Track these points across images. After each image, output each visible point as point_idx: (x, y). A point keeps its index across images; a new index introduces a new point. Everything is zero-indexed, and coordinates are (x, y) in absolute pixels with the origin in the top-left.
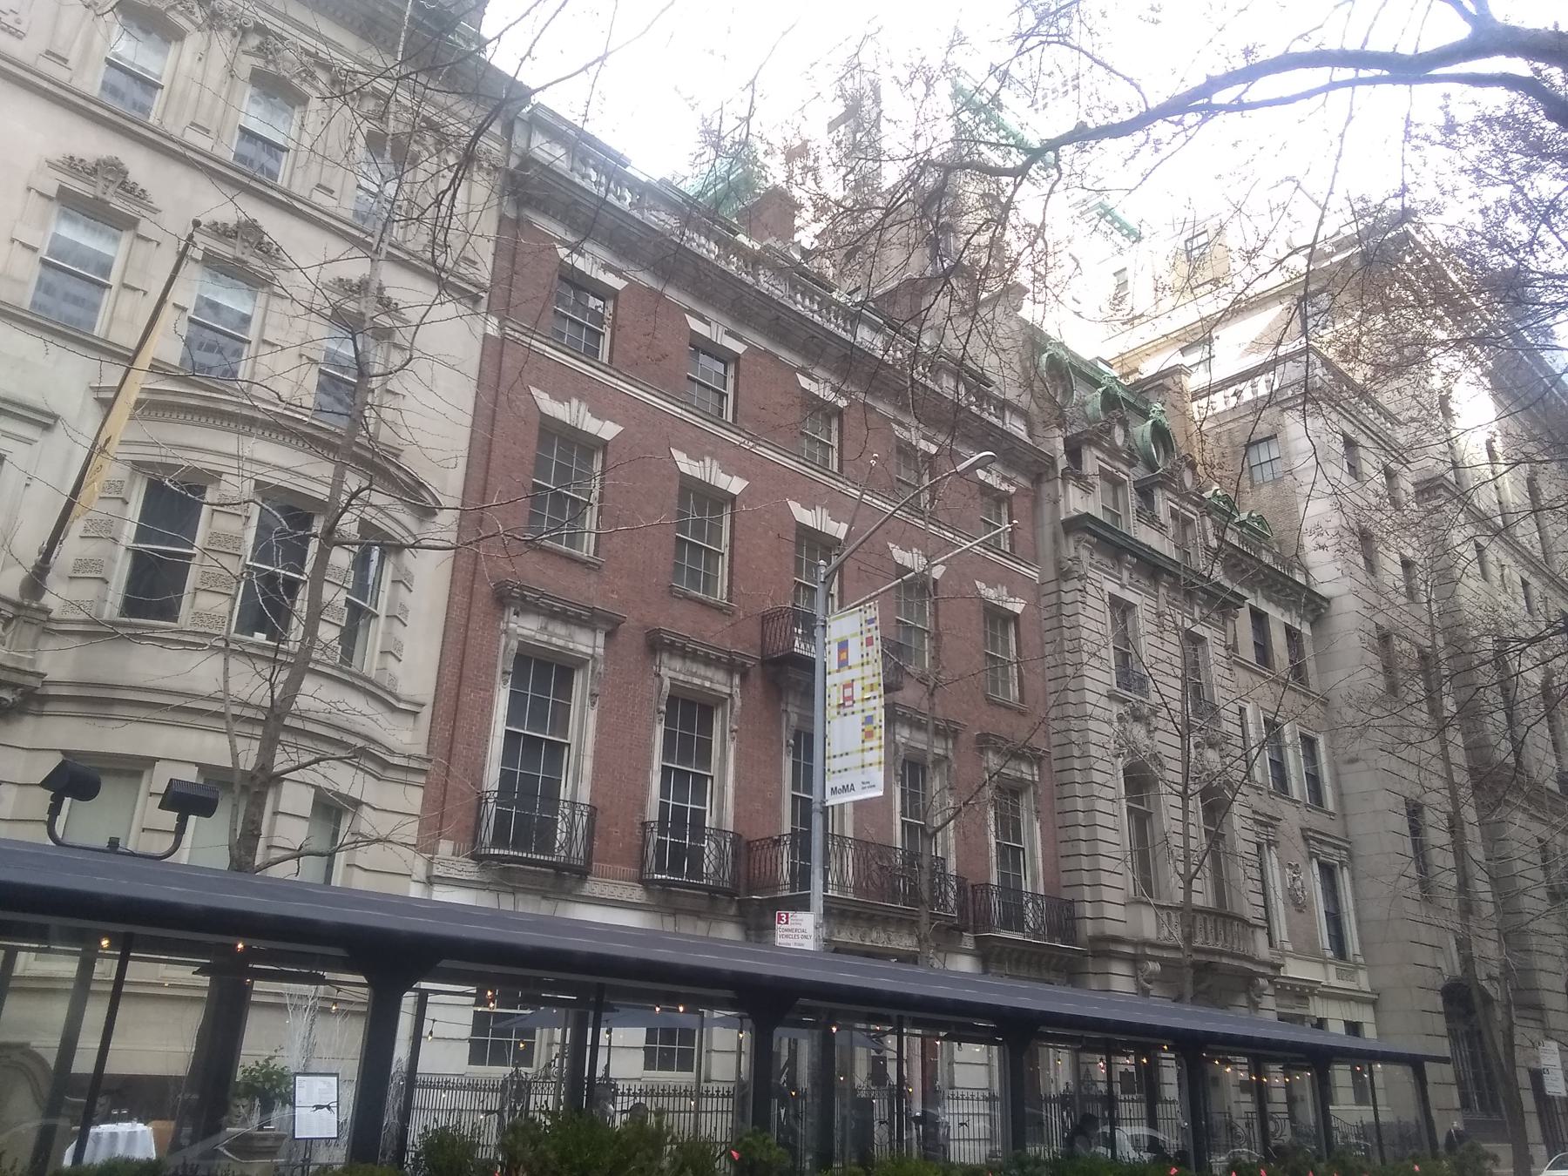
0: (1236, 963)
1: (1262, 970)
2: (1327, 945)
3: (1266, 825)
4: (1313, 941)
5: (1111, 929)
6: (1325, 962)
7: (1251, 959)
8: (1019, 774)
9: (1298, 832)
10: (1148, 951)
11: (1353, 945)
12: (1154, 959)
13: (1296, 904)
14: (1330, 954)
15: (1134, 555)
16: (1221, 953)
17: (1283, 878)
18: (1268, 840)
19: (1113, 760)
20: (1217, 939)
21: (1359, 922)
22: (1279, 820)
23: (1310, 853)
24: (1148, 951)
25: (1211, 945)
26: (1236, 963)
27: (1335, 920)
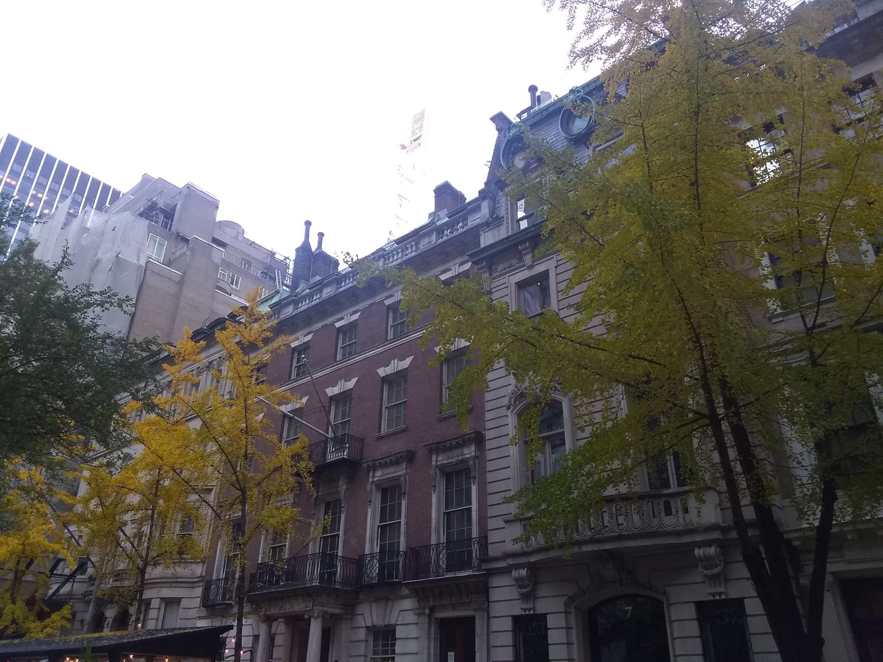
8: (460, 458)
10: (510, 561)
15: (522, 242)
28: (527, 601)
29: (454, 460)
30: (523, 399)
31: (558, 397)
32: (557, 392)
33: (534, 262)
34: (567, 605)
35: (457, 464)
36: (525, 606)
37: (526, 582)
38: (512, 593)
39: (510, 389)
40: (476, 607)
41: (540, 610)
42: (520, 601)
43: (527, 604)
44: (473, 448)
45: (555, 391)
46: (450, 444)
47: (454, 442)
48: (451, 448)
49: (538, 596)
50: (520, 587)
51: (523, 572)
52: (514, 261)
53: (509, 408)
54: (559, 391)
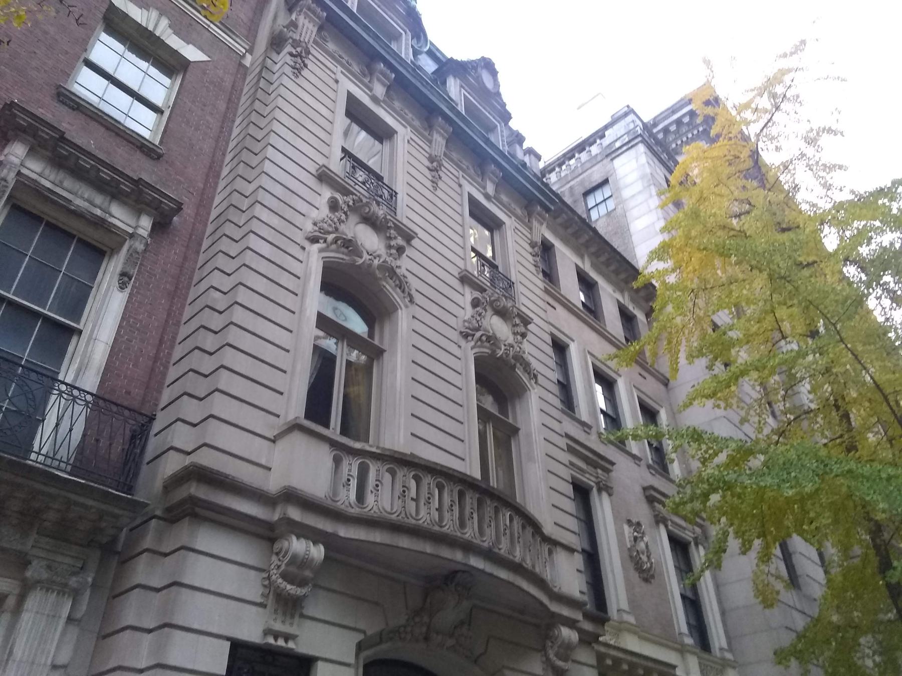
0: (503, 574)
1: (566, 612)
2: (684, 629)
3: (595, 466)
4: (668, 623)
5: (207, 459)
6: (682, 650)
7: (541, 583)
9: (638, 490)
10: (295, 514)
11: (718, 637)
12: (316, 536)
13: (638, 567)
14: (689, 641)
16: (468, 547)
17: (620, 534)
18: (598, 484)
19: (306, 244)
20: (462, 525)
21: (723, 613)
22: (613, 464)
23: (656, 516)
24: (295, 514)
25: (450, 526)
26: (503, 574)
27: (693, 603)
28: (284, 614)
29: (78, 202)
30: (345, 250)
31: (396, 296)
32: (398, 289)
33: (384, 101)
34: (360, 647)
35: (78, 214)
36: (278, 626)
37: (308, 573)
38: (252, 587)
39: (314, 214)
40: (45, 575)
41: (302, 646)
42: (260, 610)
43: (283, 622)
44: (146, 223)
45: (396, 286)
46: (92, 166)
47: (106, 174)
48: (78, 173)
49: (305, 612)
50: (285, 576)
51: (318, 552)
52: (356, 68)
53: (314, 240)
54: (403, 292)
